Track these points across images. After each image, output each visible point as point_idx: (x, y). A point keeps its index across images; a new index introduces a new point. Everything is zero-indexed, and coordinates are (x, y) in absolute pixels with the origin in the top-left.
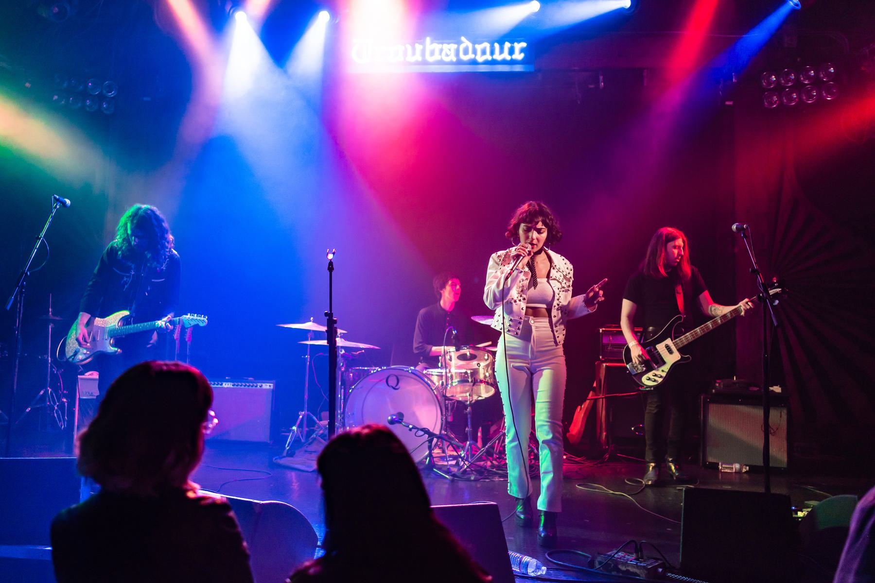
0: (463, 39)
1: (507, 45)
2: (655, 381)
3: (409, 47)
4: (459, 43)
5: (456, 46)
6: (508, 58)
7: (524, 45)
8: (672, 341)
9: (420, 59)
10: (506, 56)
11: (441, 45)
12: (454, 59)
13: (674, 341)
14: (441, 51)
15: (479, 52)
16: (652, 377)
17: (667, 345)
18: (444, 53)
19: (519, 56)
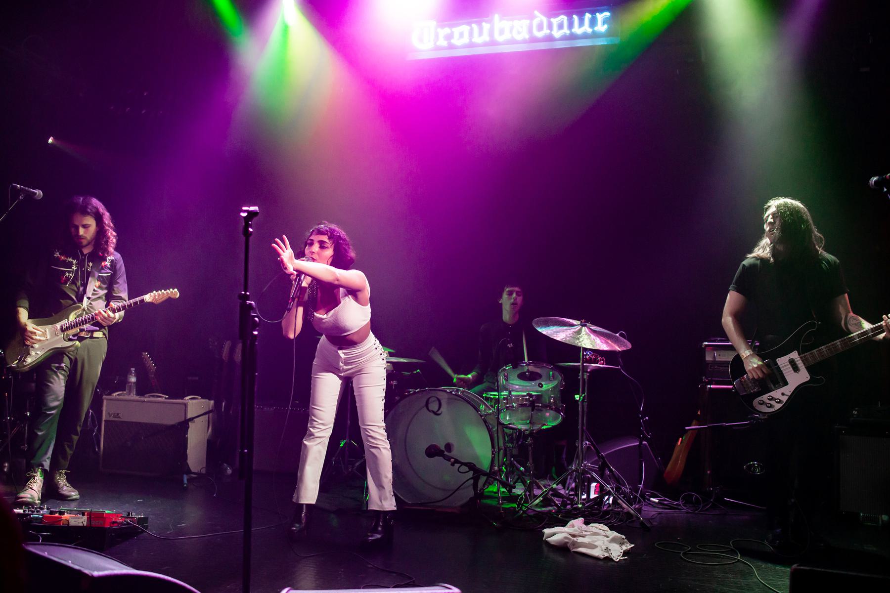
1: (588, 16)
3: (474, 26)
5: (528, 21)
6: (590, 30)
10: (587, 28)
12: (527, 37)
15: (555, 27)
19: (601, 28)
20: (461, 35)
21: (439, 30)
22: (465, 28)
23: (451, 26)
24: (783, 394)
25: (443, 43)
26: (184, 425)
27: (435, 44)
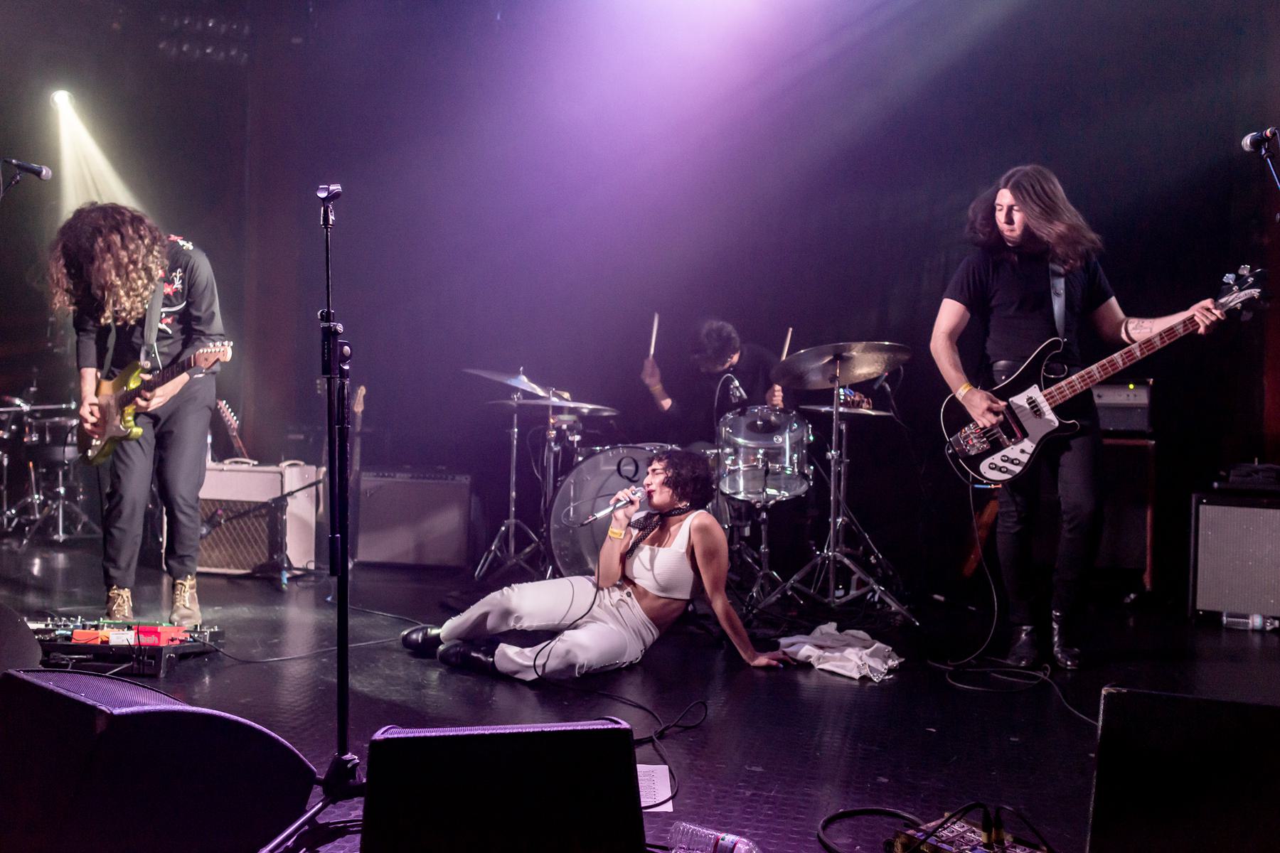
2: (1007, 471)
8: (1041, 390)
13: (1046, 392)
16: (1001, 464)
17: (1031, 398)
24: (1023, 451)
26: (279, 504)
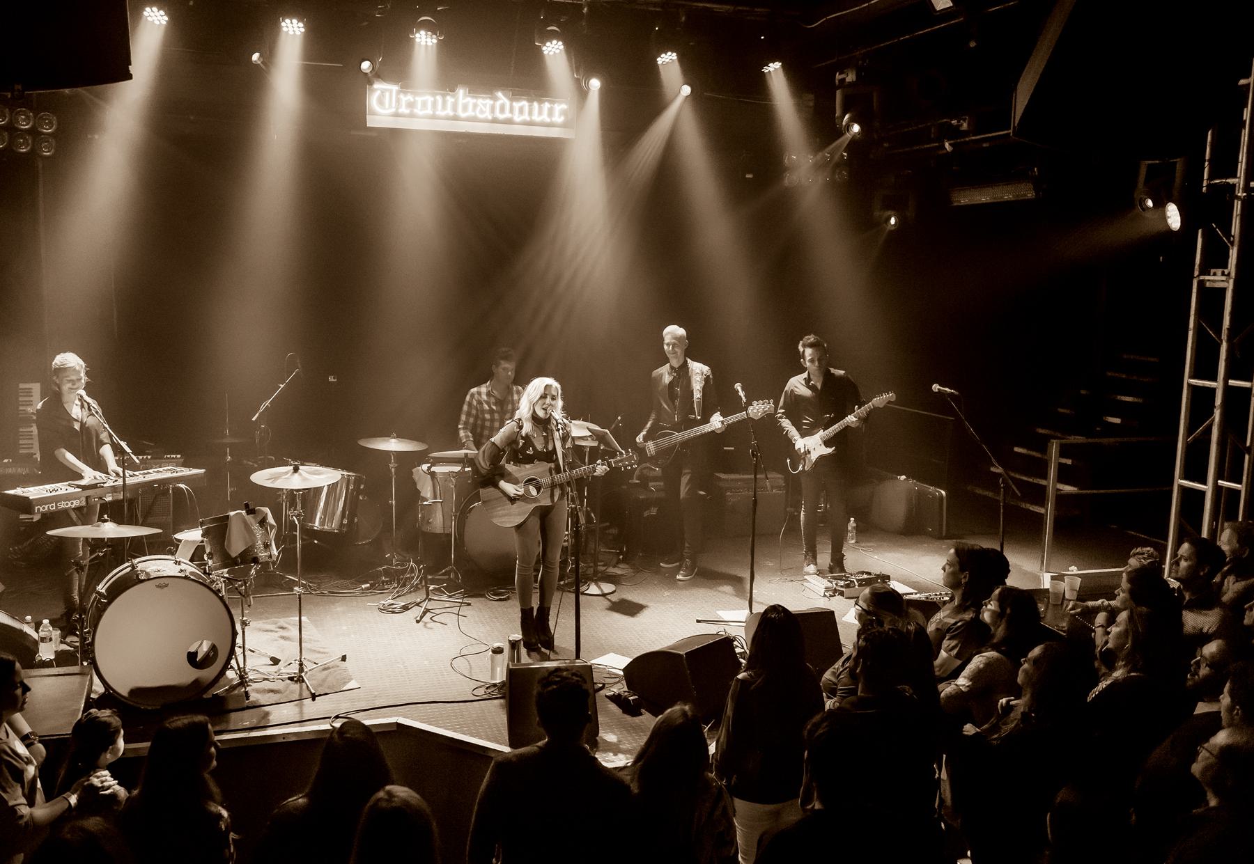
0: (500, 94)
3: (439, 98)
4: (495, 99)
5: (492, 102)
6: (548, 120)
7: (564, 106)
9: (451, 114)
11: (475, 101)
12: (490, 118)
14: (475, 106)
18: (479, 109)
19: (557, 118)
20: (424, 104)
21: (402, 96)
22: (430, 99)
23: (415, 94)
25: (404, 110)
27: (397, 109)
